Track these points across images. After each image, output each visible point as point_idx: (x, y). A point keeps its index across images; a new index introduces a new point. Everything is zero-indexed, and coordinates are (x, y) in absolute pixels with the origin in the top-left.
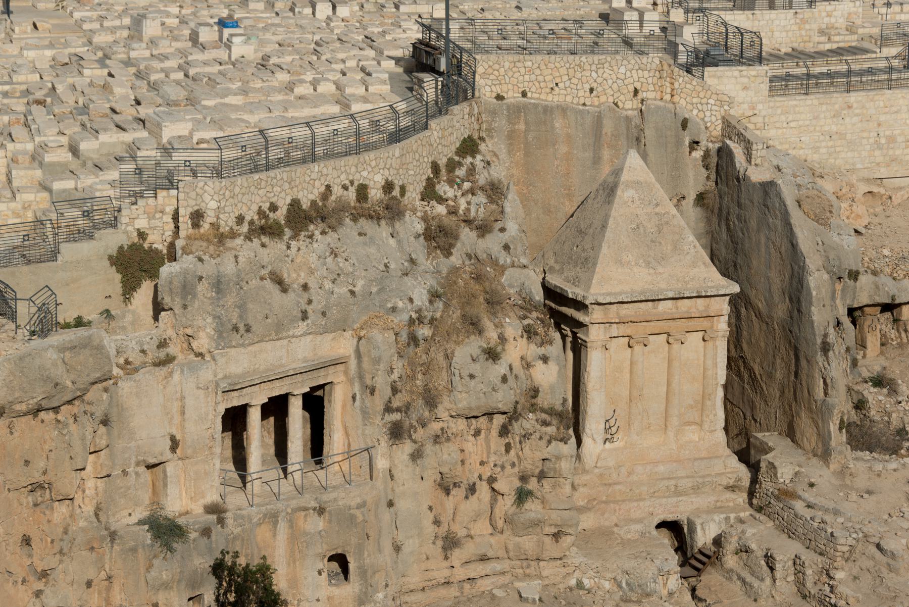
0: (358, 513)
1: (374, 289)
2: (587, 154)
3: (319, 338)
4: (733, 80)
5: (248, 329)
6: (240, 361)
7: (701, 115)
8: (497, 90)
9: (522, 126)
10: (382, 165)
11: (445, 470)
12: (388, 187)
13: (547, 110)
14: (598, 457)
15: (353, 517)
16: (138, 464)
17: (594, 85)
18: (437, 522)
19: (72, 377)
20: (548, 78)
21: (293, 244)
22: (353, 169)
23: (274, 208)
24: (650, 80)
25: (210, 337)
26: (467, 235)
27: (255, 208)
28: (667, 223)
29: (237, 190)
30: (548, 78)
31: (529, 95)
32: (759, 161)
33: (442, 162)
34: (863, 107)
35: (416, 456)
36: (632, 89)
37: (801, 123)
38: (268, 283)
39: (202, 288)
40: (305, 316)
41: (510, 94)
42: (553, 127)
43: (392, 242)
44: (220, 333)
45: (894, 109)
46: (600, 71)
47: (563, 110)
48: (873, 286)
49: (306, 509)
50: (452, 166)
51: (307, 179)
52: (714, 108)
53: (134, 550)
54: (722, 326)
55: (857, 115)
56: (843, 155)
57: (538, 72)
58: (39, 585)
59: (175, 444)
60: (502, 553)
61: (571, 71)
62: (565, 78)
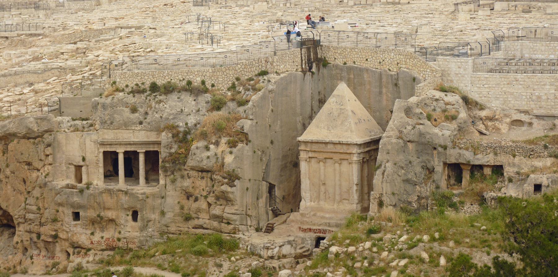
0: (140, 196)
1: (171, 117)
2: (377, 90)
3: (149, 133)
4: (454, 64)
5: (112, 123)
6: (109, 135)
7: (424, 76)
8: (345, 60)
9: (352, 76)
10: (200, 74)
11: (184, 188)
12: (203, 83)
13: (361, 70)
14: (306, 208)
15: (138, 197)
16: (70, 164)
17: (381, 61)
18: (182, 208)
19: (39, 128)
20: (364, 56)
21: (148, 97)
22: (185, 74)
23: (143, 84)
24: (403, 60)
25: (99, 125)
26: (232, 105)
27: (135, 83)
28: (343, 113)
29: (127, 76)
30: (364, 56)
31: (356, 63)
32: (418, 94)
33: (244, 78)
34: (524, 81)
35: (173, 181)
36: (396, 62)
37: (490, 86)
38: (127, 110)
39: (99, 107)
40: (141, 123)
41: (349, 62)
42: (363, 77)
43: (193, 103)
44: (102, 123)
45: (542, 83)
46: (384, 55)
47: (367, 70)
48: (458, 155)
49: (123, 191)
50: (251, 79)
51: (162, 75)
52: (430, 73)
53: (51, 190)
54: (355, 158)
55: (521, 85)
56: (513, 102)
57: (360, 54)
58: (27, 196)
59: (84, 159)
60: (209, 227)
61: (373, 54)
62: (370, 57)
